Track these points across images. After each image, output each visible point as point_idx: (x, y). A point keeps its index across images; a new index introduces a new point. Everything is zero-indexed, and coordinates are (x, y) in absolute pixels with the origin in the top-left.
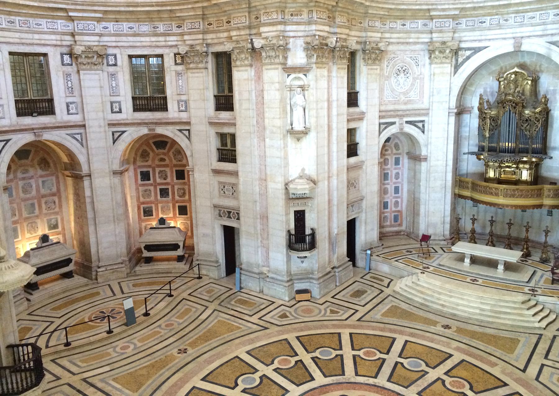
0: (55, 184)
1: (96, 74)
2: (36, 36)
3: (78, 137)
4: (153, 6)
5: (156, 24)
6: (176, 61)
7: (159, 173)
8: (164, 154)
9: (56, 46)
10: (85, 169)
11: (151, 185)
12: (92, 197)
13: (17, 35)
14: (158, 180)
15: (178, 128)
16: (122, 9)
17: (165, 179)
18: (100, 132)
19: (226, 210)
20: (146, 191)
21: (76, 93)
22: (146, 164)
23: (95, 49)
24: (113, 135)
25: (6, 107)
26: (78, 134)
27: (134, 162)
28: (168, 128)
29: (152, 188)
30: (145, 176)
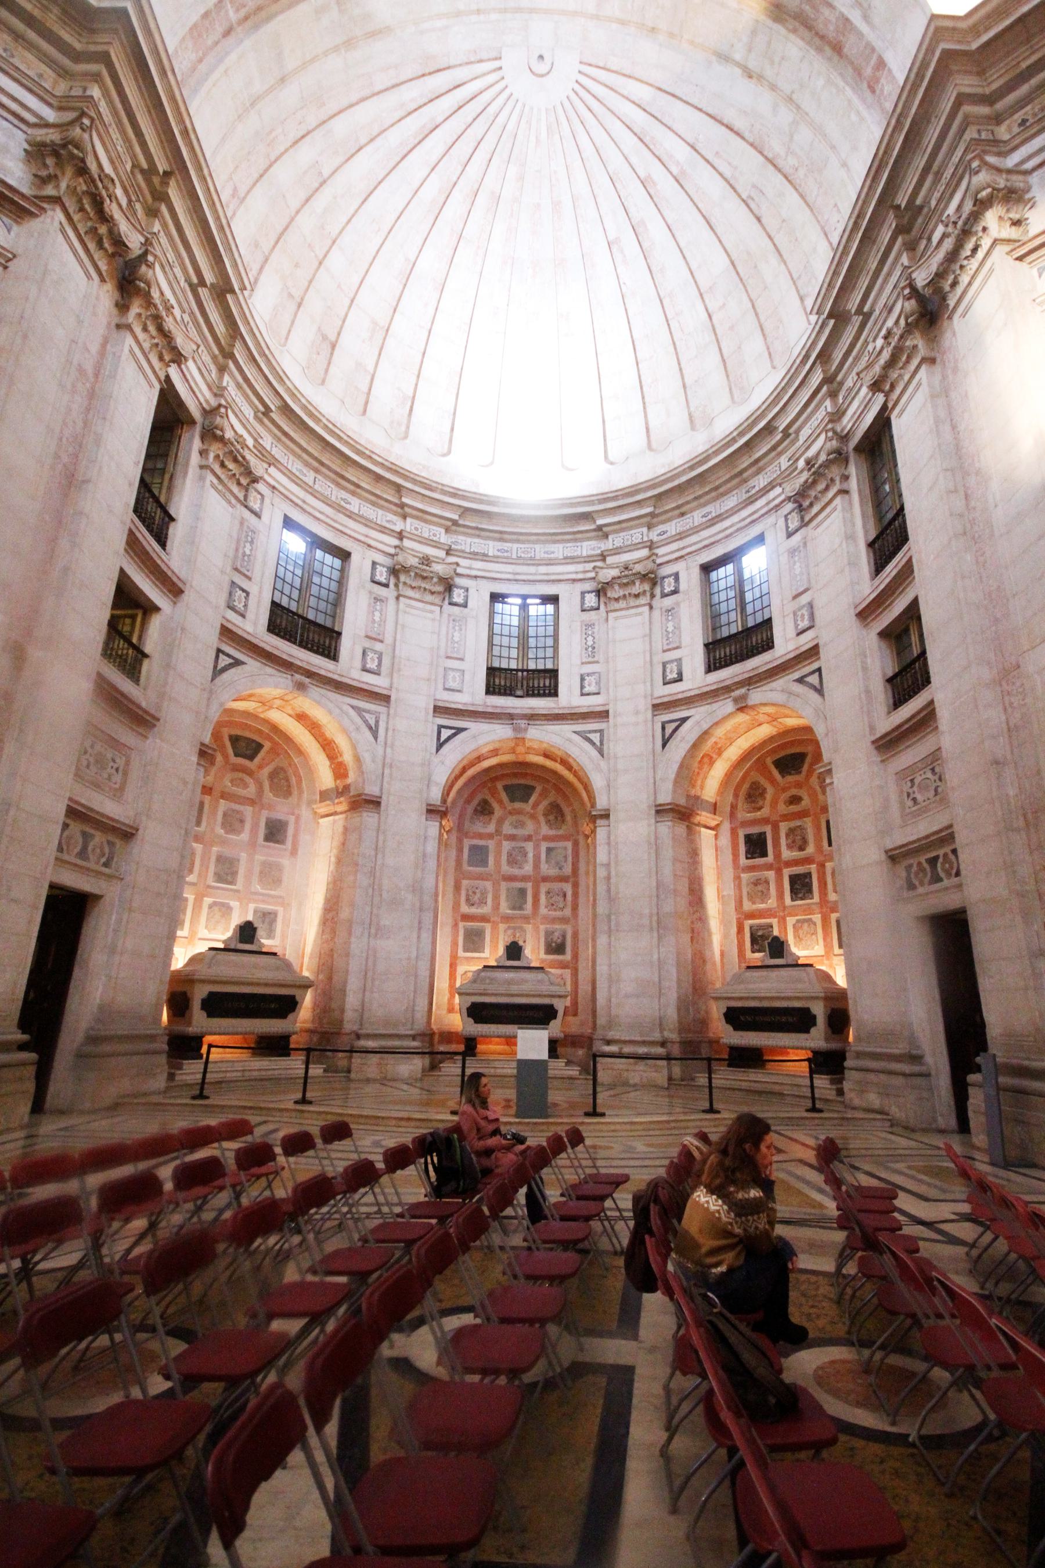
0: (570, 859)
1: (637, 615)
2: (543, 569)
3: (596, 738)
4: (734, 440)
5: (751, 483)
6: (787, 527)
7: (787, 836)
8: (799, 785)
9: (574, 580)
10: (601, 802)
11: (769, 867)
12: (608, 866)
13: (510, 568)
14: (787, 854)
15: (797, 675)
16: (684, 479)
17: (801, 849)
18: (637, 724)
19: (923, 859)
20: (756, 883)
21: (600, 656)
22: (758, 814)
23: (638, 568)
24: (663, 728)
25: (467, 677)
26: (595, 731)
27: (732, 815)
28: (774, 685)
29: (771, 875)
30: (756, 846)
